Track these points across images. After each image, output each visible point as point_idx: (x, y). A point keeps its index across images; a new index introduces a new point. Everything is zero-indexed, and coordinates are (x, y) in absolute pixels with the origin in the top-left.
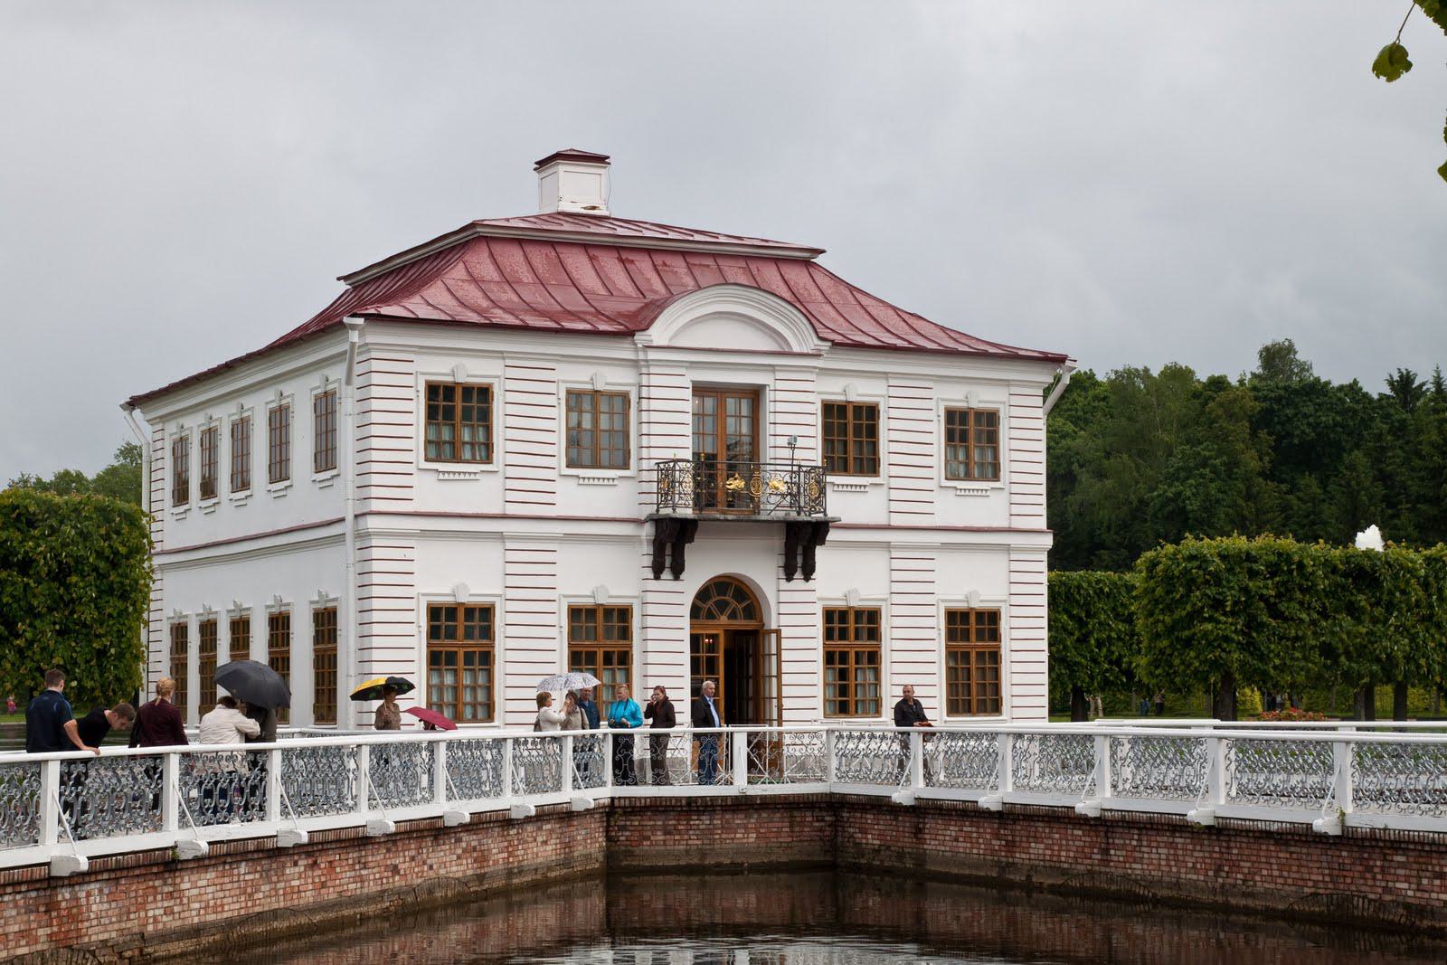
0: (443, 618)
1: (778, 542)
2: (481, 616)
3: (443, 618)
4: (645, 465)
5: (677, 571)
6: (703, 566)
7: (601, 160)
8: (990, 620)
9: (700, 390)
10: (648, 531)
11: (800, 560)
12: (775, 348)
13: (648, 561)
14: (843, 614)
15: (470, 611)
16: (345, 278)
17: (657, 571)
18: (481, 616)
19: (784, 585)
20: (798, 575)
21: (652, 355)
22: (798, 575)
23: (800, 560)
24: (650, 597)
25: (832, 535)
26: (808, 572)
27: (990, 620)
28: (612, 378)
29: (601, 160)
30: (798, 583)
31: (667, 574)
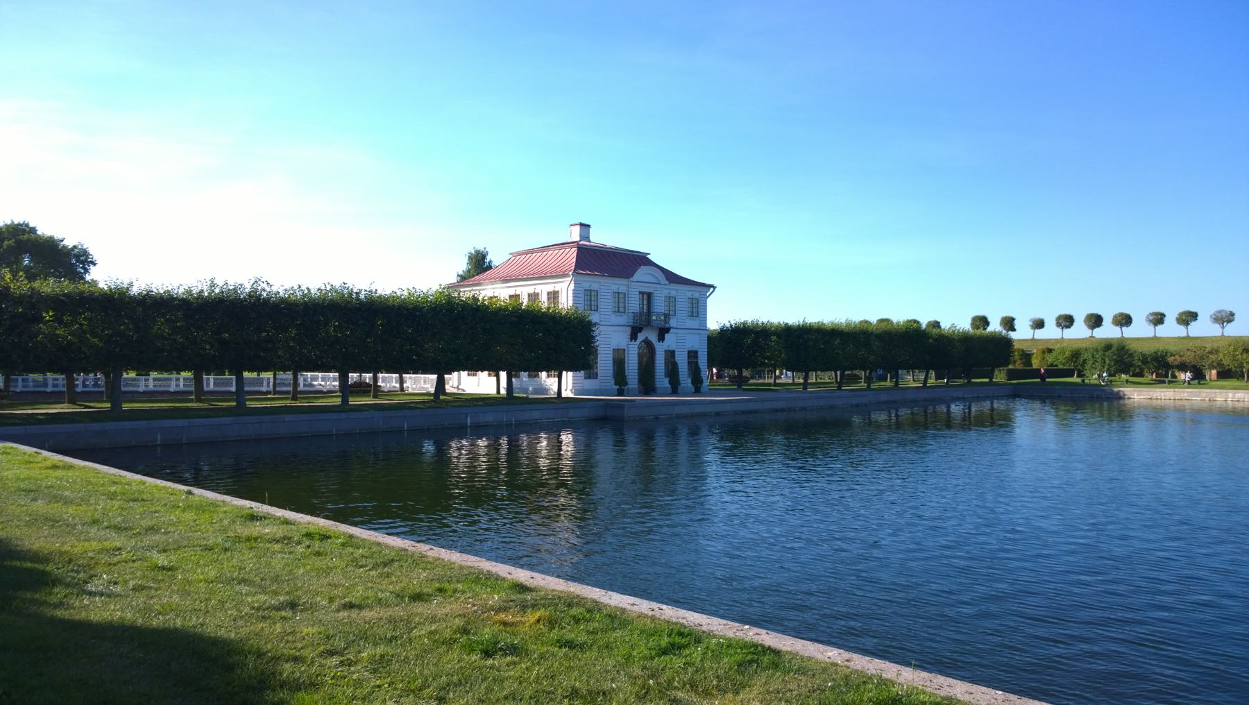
4: (630, 311)
6: (641, 337)
7: (572, 225)
8: (696, 352)
9: (640, 293)
10: (629, 329)
12: (656, 282)
13: (629, 337)
16: (510, 254)
19: (659, 344)
21: (632, 283)
24: (630, 346)
25: (672, 330)
27: (696, 352)
28: (623, 289)
29: (572, 225)
30: (661, 343)
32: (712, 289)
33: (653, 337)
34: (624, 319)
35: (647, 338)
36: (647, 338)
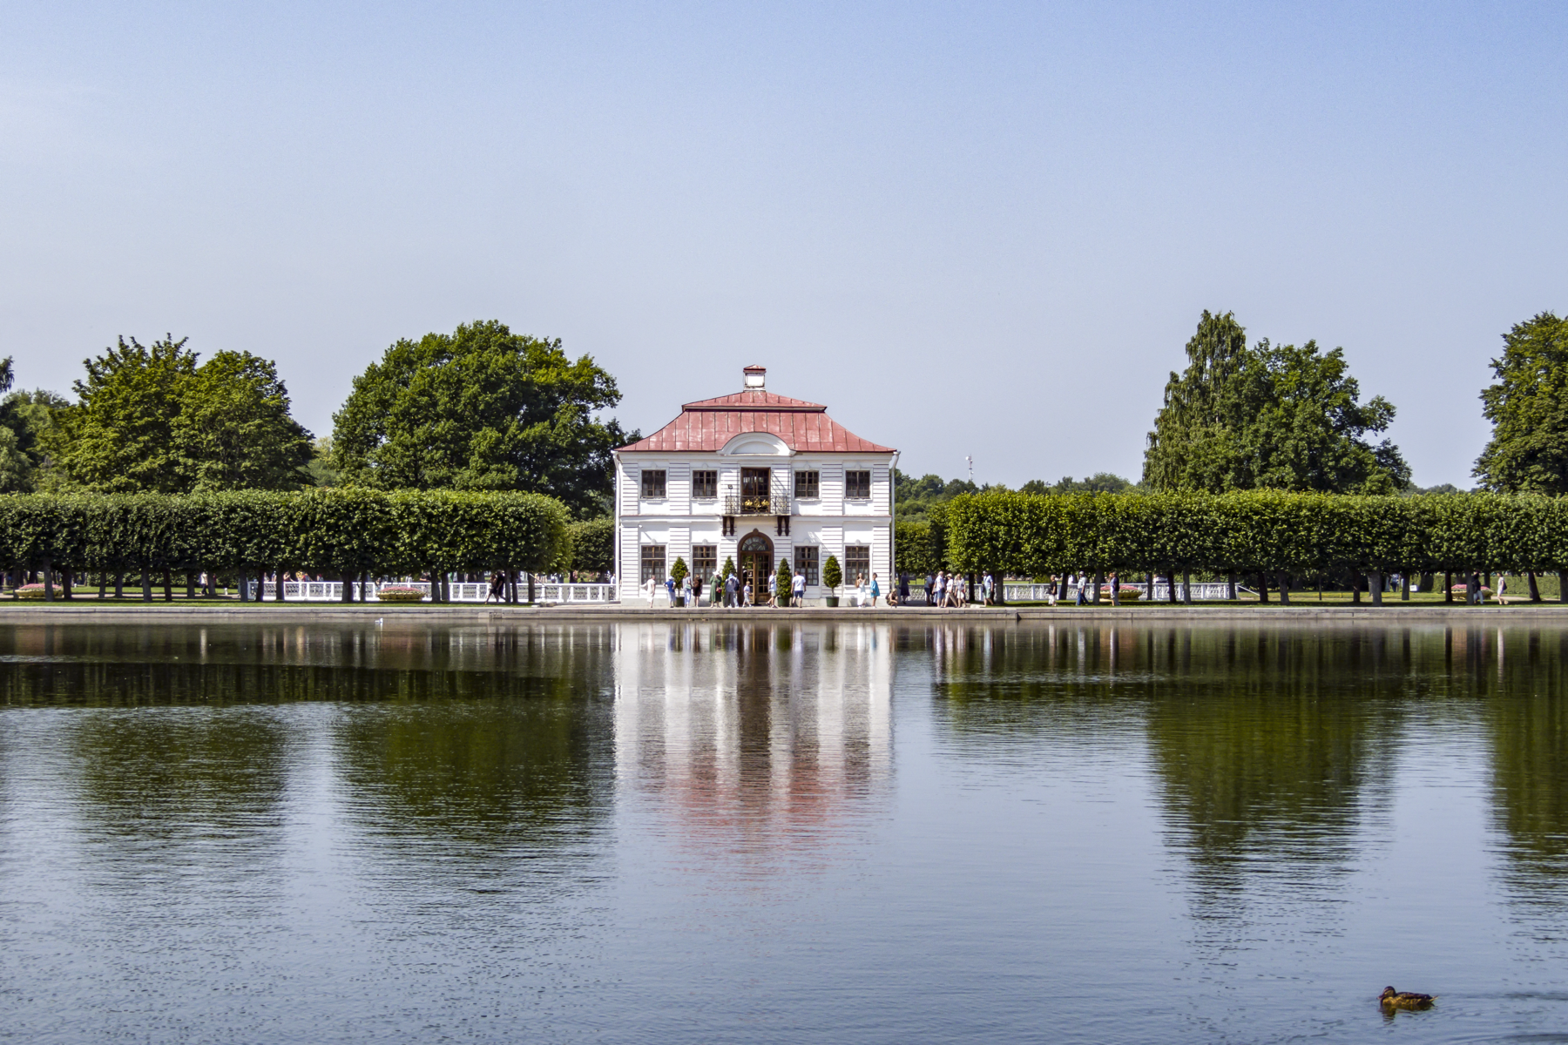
0: (646, 550)
1: (775, 523)
2: (660, 550)
3: (646, 550)
5: (732, 532)
11: (783, 529)
13: (721, 529)
14: (650, 548)
15: (656, 548)
17: (725, 533)
18: (660, 550)
20: (784, 533)
22: (784, 533)
23: (783, 529)
26: (787, 534)
28: (710, 467)
31: (728, 533)
32: (894, 458)
33: (769, 529)
34: (718, 508)
35: (756, 530)
36: (756, 530)
